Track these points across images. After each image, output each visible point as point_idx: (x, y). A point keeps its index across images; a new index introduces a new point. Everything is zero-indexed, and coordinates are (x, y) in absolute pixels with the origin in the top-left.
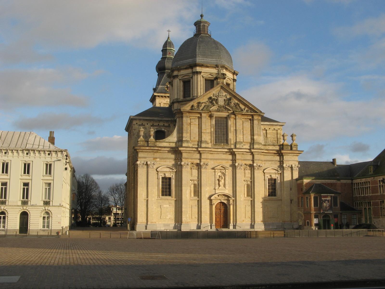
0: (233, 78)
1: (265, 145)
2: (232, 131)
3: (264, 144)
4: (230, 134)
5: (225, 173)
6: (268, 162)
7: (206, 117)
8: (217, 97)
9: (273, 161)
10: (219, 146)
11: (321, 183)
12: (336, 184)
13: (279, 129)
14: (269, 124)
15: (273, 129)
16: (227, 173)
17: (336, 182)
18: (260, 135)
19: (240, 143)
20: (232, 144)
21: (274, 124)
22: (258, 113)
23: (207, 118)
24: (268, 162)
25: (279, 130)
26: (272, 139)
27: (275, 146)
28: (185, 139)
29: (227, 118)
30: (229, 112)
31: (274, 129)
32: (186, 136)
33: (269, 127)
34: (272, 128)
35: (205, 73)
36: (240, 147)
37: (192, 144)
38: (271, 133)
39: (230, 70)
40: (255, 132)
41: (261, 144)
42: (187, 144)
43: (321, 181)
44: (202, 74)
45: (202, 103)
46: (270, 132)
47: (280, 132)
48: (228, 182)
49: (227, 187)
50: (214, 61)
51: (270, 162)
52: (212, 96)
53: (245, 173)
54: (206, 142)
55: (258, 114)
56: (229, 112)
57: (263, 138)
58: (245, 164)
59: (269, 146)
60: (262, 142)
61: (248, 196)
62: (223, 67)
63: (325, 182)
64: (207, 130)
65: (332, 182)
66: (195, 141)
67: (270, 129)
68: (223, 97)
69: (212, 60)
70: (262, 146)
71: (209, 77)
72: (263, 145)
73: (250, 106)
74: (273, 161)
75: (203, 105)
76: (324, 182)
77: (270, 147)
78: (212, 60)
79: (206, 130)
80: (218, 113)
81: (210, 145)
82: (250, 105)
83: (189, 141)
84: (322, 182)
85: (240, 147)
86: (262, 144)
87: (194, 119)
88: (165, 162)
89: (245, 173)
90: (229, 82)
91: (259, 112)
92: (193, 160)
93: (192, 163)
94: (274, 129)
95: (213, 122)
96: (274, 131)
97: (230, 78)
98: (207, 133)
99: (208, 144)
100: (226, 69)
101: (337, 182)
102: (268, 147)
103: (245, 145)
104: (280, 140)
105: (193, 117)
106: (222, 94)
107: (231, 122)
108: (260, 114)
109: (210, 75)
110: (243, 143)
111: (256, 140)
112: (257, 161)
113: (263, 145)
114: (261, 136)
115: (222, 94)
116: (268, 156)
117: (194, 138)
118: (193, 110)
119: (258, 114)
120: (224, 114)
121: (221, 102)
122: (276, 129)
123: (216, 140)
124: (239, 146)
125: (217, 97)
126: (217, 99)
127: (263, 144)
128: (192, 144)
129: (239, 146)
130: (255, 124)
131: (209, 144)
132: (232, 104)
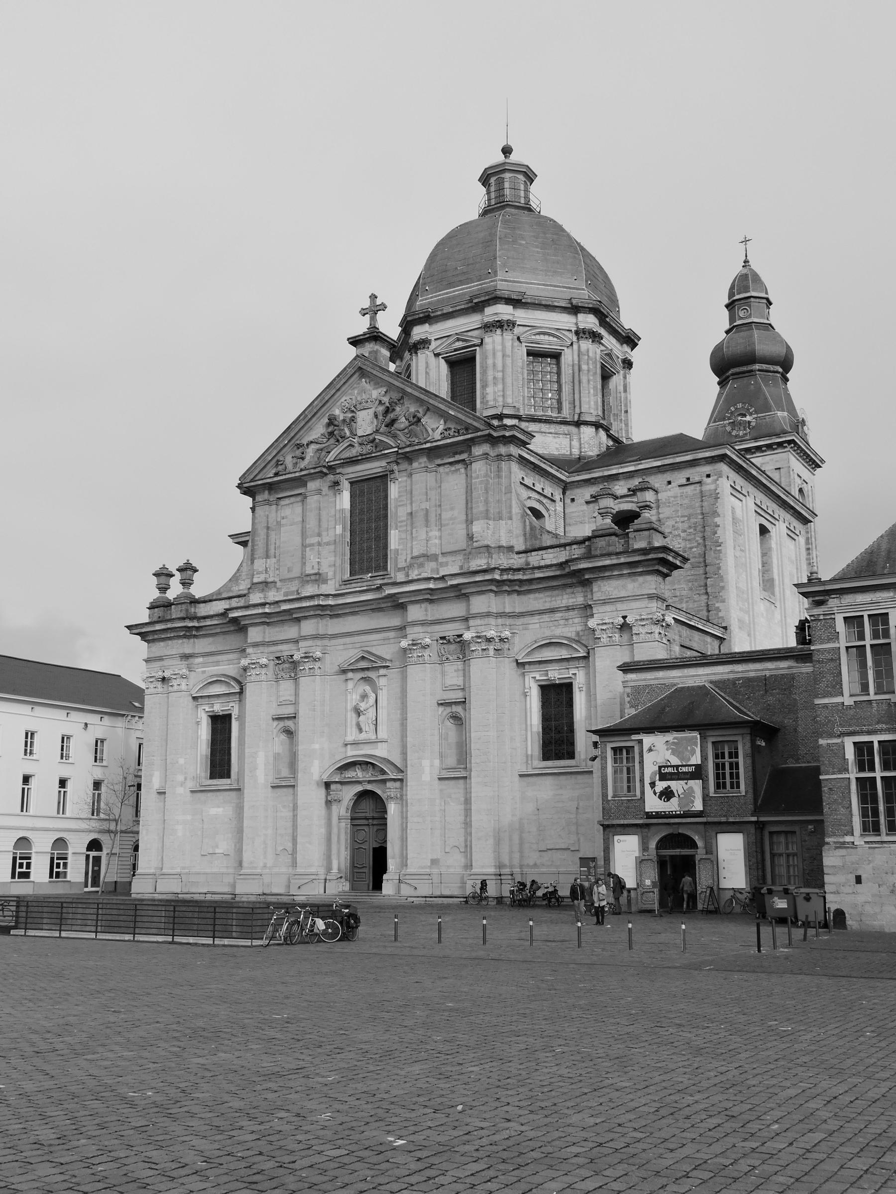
0: (574, 329)
1: (525, 552)
2: (402, 522)
3: (523, 548)
4: (392, 532)
5: (376, 680)
6: (536, 619)
7: (319, 492)
8: (353, 412)
9: (552, 611)
10: (359, 584)
11: (711, 682)
12: (792, 677)
13: (708, 476)
14: (659, 463)
15: (684, 481)
16: (382, 682)
17: (789, 668)
18: (505, 514)
19: (422, 559)
20: (400, 570)
21: (678, 460)
22: (478, 430)
23: (324, 493)
24: (537, 617)
25: (709, 480)
26: (683, 522)
27: (567, 547)
28: (260, 580)
29: (383, 479)
30: (386, 452)
31: (688, 479)
32: (260, 570)
33: (668, 476)
34: (680, 477)
35: (445, 339)
36: (420, 575)
37: (283, 591)
38: (675, 497)
39: (544, 303)
40: (479, 508)
41: (510, 549)
42: (262, 595)
43: (707, 675)
44: (433, 345)
45: (308, 445)
46: (669, 494)
47: (712, 487)
48: (389, 715)
49: (383, 734)
50: (474, 286)
51: (546, 617)
52: (337, 412)
53: (443, 674)
54: (319, 578)
55: (479, 434)
56: (386, 452)
57: (520, 525)
58: (443, 638)
59: (540, 552)
60: (513, 542)
61: (459, 762)
62: (495, 299)
63: (731, 676)
64: (324, 534)
65: (768, 673)
66: (291, 580)
67: (669, 483)
68: (369, 405)
69: (467, 288)
70: (516, 556)
71: (456, 350)
72: (518, 553)
73: (450, 412)
74: (552, 611)
75: (310, 452)
76: (726, 677)
77: (545, 556)
78: (467, 288)
79: (319, 535)
80: (359, 468)
81: (329, 588)
82: (450, 408)
83: (275, 582)
84: (714, 678)
85: (420, 575)
86: (516, 549)
87: (291, 506)
88: (217, 663)
89: (443, 674)
90: (547, 343)
91: (482, 427)
92: (280, 647)
93: (278, 658)
94: (688, 479)
95: (345, 500)
96: (689, 489)
97: (550, 328)
98: (324, 543)
99: (325, 581)
100: (516, 303)
101: (794, 671)
102: (539, 558)
103: (447, 564)
104: (717, 520)
105: (287, 501)
106: (364, 396)
107: (394, 490)
108: (487, 432)
109: (458, 340)
110: (441, 559)
111: (478, 539)
112: (478, 622)
113: (518, 553)
114: (511, 518)
115: (364, 396)
116: (537, 595)
117: (289, 570)
118: (276, 474)
119: (479, 434)
120: (374, 467)
121: (365, 423)
122: (697, 479)
123: (351, 564)
124: (416, 572)
125: (353, 412)
126: (353, 419)
127: (520, 545)
128: (283, 591)
129: (416, 572)
130: (477, 477)
131: (329, 582)
132: (402, 423)
